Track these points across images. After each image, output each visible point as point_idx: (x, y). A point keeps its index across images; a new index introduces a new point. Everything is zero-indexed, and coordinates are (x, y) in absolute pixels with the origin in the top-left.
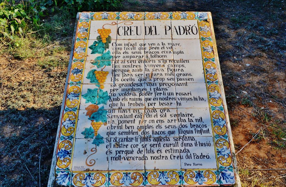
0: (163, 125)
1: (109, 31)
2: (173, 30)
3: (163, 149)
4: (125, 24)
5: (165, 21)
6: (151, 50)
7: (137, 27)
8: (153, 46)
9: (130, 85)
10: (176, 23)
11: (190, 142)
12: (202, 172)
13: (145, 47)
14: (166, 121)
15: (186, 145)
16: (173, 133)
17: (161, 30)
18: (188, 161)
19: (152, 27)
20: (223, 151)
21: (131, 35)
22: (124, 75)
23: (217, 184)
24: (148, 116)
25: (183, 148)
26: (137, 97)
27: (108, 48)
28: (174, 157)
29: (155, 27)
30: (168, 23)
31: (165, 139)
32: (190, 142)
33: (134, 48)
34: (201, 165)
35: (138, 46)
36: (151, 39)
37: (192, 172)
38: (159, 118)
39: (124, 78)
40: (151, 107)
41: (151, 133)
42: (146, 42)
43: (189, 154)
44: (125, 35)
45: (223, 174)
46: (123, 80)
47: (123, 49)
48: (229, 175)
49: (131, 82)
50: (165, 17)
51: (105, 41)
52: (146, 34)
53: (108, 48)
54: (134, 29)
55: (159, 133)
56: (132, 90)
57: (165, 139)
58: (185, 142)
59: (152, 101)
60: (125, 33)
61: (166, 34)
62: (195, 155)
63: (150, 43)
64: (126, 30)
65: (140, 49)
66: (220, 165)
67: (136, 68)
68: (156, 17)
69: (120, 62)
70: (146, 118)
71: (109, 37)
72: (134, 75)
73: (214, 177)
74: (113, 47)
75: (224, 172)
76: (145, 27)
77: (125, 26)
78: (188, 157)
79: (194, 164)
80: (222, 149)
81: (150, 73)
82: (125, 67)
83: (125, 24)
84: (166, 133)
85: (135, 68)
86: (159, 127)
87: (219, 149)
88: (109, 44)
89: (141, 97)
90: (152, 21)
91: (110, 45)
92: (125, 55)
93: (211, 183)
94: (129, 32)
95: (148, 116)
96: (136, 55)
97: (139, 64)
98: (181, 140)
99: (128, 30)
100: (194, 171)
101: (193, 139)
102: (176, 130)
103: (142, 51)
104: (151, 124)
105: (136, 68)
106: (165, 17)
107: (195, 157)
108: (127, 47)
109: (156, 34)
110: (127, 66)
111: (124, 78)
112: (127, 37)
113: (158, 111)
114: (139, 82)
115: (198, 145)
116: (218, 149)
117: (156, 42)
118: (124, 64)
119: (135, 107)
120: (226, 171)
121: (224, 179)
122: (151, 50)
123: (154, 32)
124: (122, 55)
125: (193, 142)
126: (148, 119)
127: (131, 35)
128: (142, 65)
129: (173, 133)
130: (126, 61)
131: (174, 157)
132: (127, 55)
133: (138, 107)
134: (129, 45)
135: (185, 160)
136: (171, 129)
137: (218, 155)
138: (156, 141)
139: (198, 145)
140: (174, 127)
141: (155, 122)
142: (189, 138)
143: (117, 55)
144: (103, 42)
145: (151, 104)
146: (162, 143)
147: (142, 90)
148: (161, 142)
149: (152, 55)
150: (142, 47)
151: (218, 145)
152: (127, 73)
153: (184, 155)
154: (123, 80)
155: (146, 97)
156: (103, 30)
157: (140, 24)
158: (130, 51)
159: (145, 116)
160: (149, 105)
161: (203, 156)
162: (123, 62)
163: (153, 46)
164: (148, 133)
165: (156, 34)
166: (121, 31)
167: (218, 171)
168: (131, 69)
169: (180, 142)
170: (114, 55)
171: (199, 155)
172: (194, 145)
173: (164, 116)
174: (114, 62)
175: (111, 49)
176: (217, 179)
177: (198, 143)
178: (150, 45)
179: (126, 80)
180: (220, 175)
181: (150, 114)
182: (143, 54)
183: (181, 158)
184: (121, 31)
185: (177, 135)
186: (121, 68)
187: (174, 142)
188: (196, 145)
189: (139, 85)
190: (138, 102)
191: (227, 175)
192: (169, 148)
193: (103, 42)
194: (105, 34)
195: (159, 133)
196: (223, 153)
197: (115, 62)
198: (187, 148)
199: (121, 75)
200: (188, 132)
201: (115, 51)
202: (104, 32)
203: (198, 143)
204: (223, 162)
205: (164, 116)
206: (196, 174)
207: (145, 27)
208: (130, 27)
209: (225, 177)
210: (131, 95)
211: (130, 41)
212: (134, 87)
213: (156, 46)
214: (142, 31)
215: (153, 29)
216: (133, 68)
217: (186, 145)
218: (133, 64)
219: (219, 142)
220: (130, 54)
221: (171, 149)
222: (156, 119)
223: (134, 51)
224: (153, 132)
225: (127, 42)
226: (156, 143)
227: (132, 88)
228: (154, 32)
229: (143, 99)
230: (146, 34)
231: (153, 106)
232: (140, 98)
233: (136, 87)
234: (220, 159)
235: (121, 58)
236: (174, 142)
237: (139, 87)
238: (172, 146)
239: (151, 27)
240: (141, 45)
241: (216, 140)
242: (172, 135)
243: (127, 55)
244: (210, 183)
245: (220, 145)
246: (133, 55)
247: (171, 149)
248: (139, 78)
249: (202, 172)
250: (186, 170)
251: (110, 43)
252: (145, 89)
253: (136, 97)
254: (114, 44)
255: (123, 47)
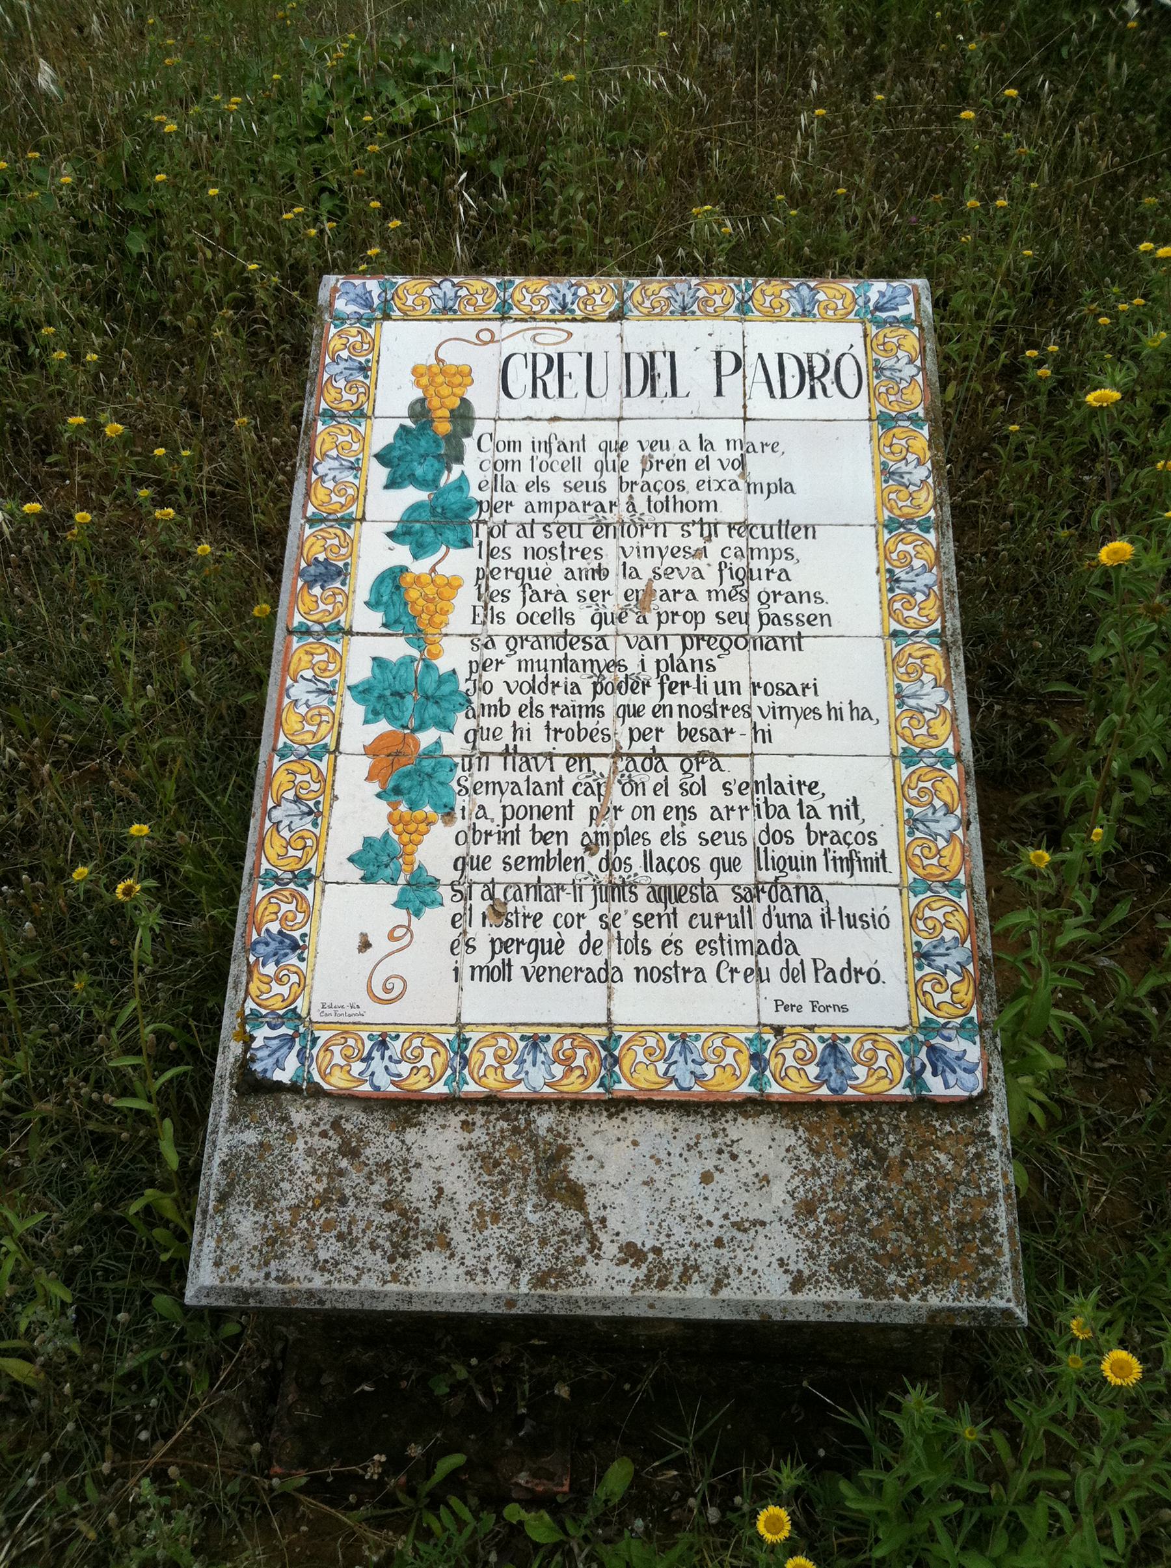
0: (691, 831)
1: (465, 375)
2: (750, 372)
3: (688, 937)
4: (534, 339)
5: (718, 325)
6: (652, 476)
7: (589, 356)
8: (658, 455)
9: (556, 646)
10: (768, 338)
11: (801, 907)
12: (848, 1040)
13: (625, 456)
14: (703, 811)
15: (784, 921)
16: (733, 865)
17: (696, 374)
18: (792, 992)
19: (659, 358)
20: (942, 950)
21: (561, 394)
22: (529, 593)
23: (907, 1092)
24: (628, 788)
25: (769, 936)
26: (585, 698)
27: (459, 459)
28: (733, 971)
29: (673, 355)
30: (727, 333)
31: (698, 891)
32: (801, 907)
33: (576, 464)
34: (844, 1009)
35: (592, 455)
36: (651, 420)
37: (806, 1040)
38: (675, 798)
39: (530, 608)
40: (641, 747)
41: (637, 862)
42: (630, 432)
43: (794, 961)
44: (534, 395)
45: (932, 1049)
46: (523, 618)
47: (526, 464)
48: (958, 1058)
49: (559, 629)
50: (719, 303)
51: (444, 427)
52: (628, 394)
53: (459, 459)
54: (575, 365)
55: (674, 865)
56: (565, 665)
57: (698, 891)
58: (782, 908)
59: (646, 721)
60: (537, 386)
61: (719, 393)
62: (820, 965)
63: (649, 436)
64: (541, 370)
65: (601, 467)
66: (924, 1013)
67: (583, 564)
68: (676, 306)
69: (511, 530)
70: (617, 798)
71: (464, 401)
72: (571, 596)
73: (894, 1064)
74: (483, 456)
75: (937, 1041)
76: (628, 356)
77: (538, 349)
78: (791, 975)
79: (814, 1005)
80: (935, 941)
81: (640, 585)
82: (536, 554)
83: (534, 339)
84: (704, 863)
85: (577, 563)
86: (675, 837)
87: (924, 942)
88: (465, 441)
89: (601, 699)
90: (657, 324)
91: (469, 443)
92: (535, 497)
93: (882, 1086)
94: (552, 380)
95: (628, 788)
96: (580, 497)
97: (593, 543)
98: (764, 897)
99: (549, 370)
100: (814, 1037)
101: (812, 893)
102: (746, 855)
103: (611, 479)
104: (639, 826)
105: (583, 564)
106: (719, 303)
107: (822, 974)
108: (543, 456)
109: (674, 394)
110: (542, 553)
111: (530, 608)
112: (544, 407)
113: (672, 764)
114: (593, 630)
115: (836, 925)
116: (918, 944)
117: (672, 432)
118: (528, 542)
119: (576, 747)
120: (949, 1039)
121: (935, 1074)
122: (652, 476)
123: (663, 384)
124: (520, 498)
125: (814, 910)
126: (628, 803)
127: (561, 394)
128: (608, 545)
129: (733, 865)
130: (538, 529)
131: (733, 971)
132: (543, 497)
133: (586, 746)
134: (554, 446)
135: (776, 989)
136: (724, 851)
137: (920, 967)
138: (658, 900)
139: (836, 925)
140: (738, 838)
141: (659, 814)
142: (798, 889)
143: (499, 496)
144: (434, 436)
145: (643, 736)
146: (684, 910)
147: (607, 666)
148: (679, 905)
149: (655, 497)
150: (612, 456)
151: (920, 924)
152: (539, 585)
153: (773, 963)
154: (523, 618)
155: (622, 700)
156: (436, 370)
157: (599, 338)
158: (555, 479)
159: (617, 788)
160: (632, 739)
161: (852, 973)
162: (525, 530)
163: (658, 455)
164: (626, 862)
165: (674, 394)
166: (520, 377)
167: (912, 1038)
168: (558, 567)
169: (760, 907)
170: (484, 496)
171: (838, 965)
172: (816, 920)
173: (695, 789)
174: (483, 529)
175: (473, 468)
176: (907, 1074)
177: (835, 915)
178: (648, 451)
179: (537, 619)
180: (923, 1055)
181: (637, 778)
182: (612, 493)
183: (757, 974)
184: (520, 377)
185: (745, 876)
186: (518, 561)
187: (735, 909)
188: (826, 921)
189: (593, 641)
190: (589, 723)
191: (950, 1057)
192: (711, 934)
193: (434, 436)
194: (445, 391)
195: (674, 865)
196: (940, 962)
197: (490, 534)
198: (786, 933)
199: (516, 595)
200: (793, 864)
201: (490, 478)
202: (440, 379)
203: (835, 915)
204: (938, 998)
205: (695, 789)
206: (820, 1047)
207: (628, 356)
208: (560, 356)
209: (940, 1065)
210: (560, 691)
211: (558, 427)
212: (572, 654)
213: (675, 453)
214: (608, 373)
215: (662, 365)
216: (569, 563)
217: (784, 921)
218: (570, 542)
219: (928, 913)
220: (557, 494)
221: (721, 939)
222: (660, 803)
223: (573, 477)
224: (647, 857)
225: (541, 431)
226: (658, 908)
227: (561, 655)
228: (663, 384)
229: (609, 711)
230: (628, 394)
231: (653, 742)
232: (596, 703)
233: (578, 654)
234: (927, 987)
235: (517, 514)
236: (735, 909)
237: (593, 654)
238: (724, 923)
239: (652, 355)
240: (606, 447)
241: (914, 901)
242: (728, 877)
243: (543, 497)
244: (875, 1089)
245: (930, 924)
246: (569, 497)
247: (721, 939)
248: (592, 611)
249: (848, 1040)
250: (778, 1030)
251: (469, 435)
252: (616, 664)
253: (580, 700)
254: (486, 443)
255: (525, 456)
